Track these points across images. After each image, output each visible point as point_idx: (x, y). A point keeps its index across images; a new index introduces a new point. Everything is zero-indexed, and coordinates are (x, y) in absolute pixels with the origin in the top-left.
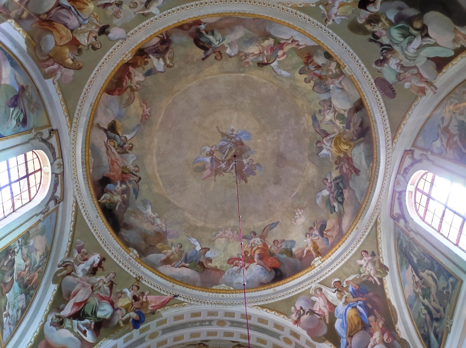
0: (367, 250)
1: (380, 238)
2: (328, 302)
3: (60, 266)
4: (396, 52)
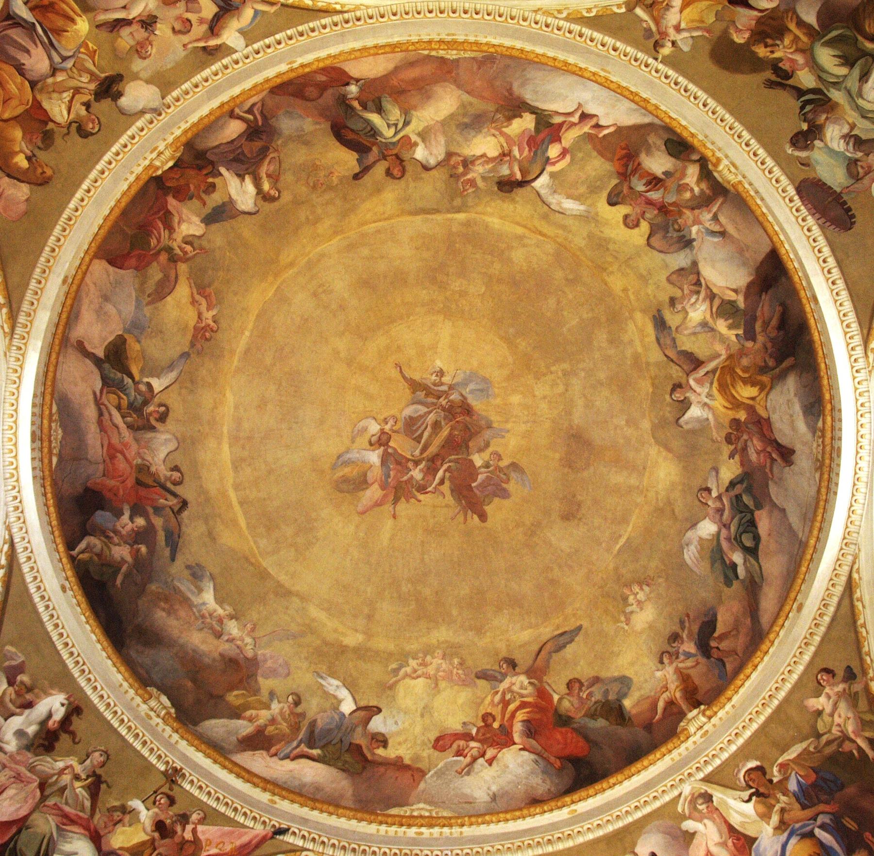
0: (830, 666)
1: (864, 625)
2: (731, 829)
4: (836, 105)
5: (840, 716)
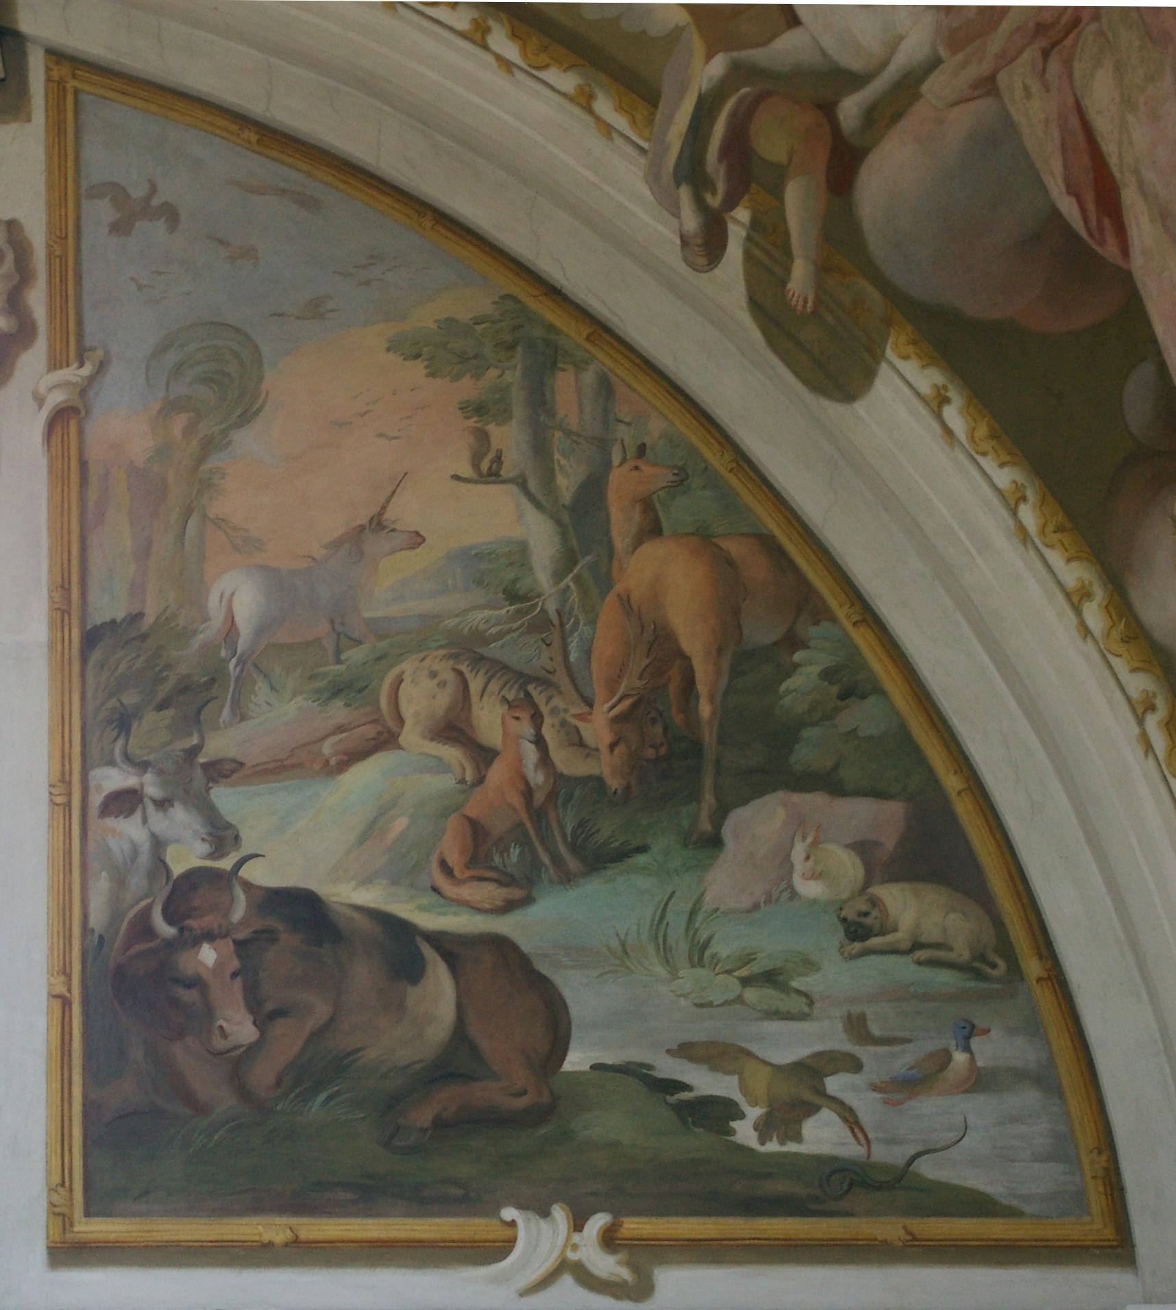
3: (711, 245)
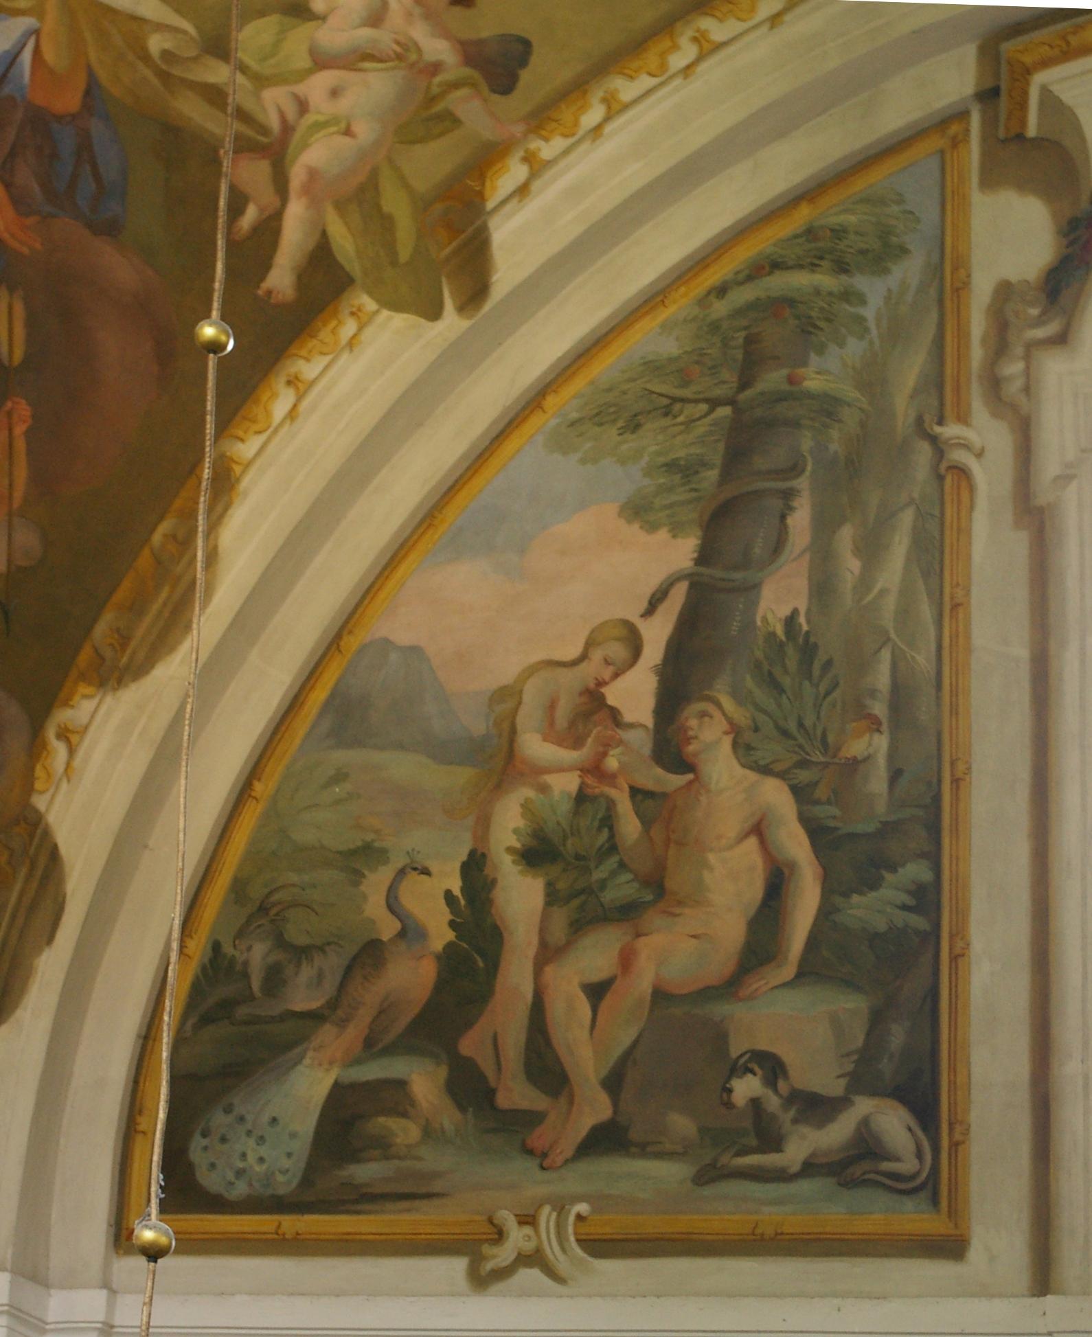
5: (335, 93)
